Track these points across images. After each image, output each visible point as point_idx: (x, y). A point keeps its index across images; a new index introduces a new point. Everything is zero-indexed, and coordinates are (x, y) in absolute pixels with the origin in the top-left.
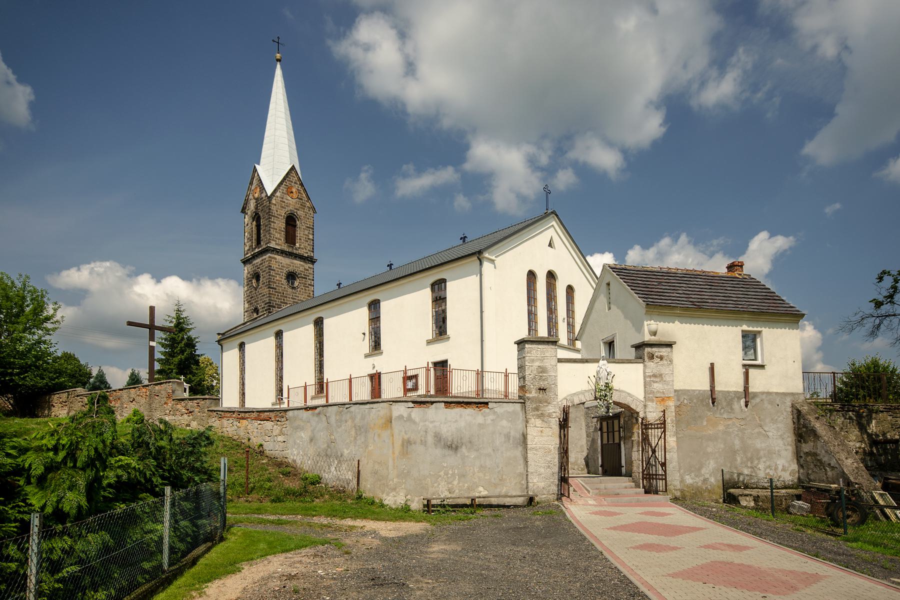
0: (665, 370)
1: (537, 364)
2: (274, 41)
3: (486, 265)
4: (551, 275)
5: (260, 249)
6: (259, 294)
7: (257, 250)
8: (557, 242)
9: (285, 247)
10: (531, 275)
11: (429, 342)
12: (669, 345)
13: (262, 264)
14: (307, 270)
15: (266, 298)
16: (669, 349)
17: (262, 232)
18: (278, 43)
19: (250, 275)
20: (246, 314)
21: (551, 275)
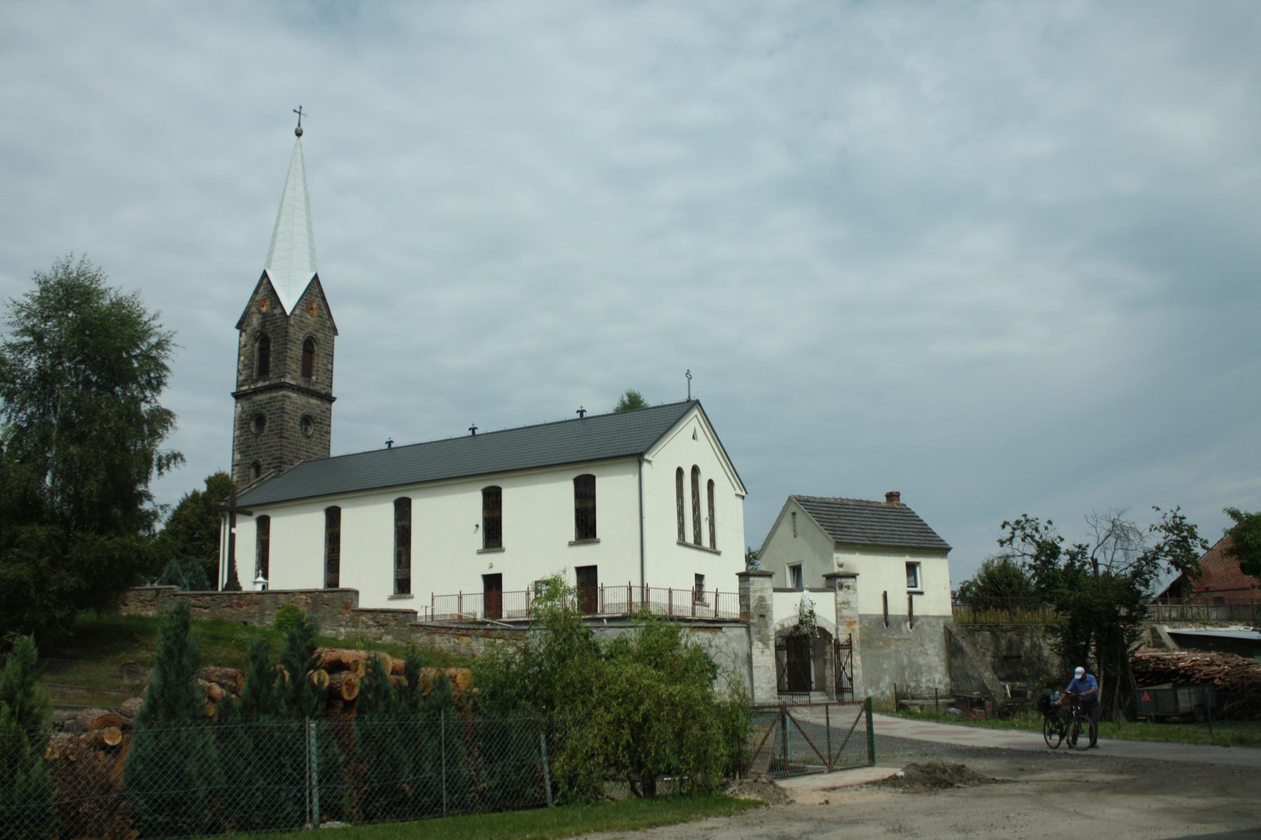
0: (851, 598)
1: (758, 594)
2: (295, 111)
3: (645, 466)
4: (695, 470)
5: (267, 383)
6: (263, 444)
7: (260, 384)
8: (700, 434)
9: (301, 382)
10: (680, 472)
11: (571, 544)
12: (854, 576)
13: (270, 403)
14: (324, 412)
15: (275, 450)
16: (853, 580)
17: (271, 359)
18: (300, 113)
19: (247, 415)
20: (236, 468)
21: (695, 470)
